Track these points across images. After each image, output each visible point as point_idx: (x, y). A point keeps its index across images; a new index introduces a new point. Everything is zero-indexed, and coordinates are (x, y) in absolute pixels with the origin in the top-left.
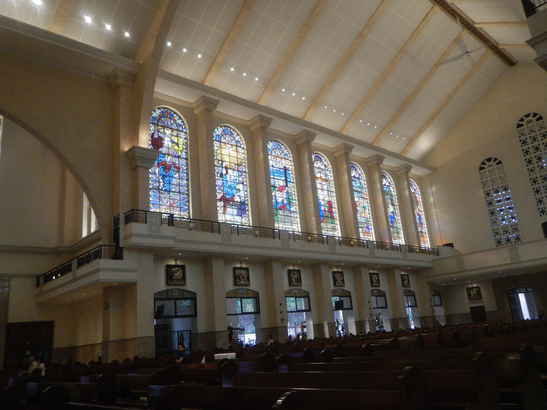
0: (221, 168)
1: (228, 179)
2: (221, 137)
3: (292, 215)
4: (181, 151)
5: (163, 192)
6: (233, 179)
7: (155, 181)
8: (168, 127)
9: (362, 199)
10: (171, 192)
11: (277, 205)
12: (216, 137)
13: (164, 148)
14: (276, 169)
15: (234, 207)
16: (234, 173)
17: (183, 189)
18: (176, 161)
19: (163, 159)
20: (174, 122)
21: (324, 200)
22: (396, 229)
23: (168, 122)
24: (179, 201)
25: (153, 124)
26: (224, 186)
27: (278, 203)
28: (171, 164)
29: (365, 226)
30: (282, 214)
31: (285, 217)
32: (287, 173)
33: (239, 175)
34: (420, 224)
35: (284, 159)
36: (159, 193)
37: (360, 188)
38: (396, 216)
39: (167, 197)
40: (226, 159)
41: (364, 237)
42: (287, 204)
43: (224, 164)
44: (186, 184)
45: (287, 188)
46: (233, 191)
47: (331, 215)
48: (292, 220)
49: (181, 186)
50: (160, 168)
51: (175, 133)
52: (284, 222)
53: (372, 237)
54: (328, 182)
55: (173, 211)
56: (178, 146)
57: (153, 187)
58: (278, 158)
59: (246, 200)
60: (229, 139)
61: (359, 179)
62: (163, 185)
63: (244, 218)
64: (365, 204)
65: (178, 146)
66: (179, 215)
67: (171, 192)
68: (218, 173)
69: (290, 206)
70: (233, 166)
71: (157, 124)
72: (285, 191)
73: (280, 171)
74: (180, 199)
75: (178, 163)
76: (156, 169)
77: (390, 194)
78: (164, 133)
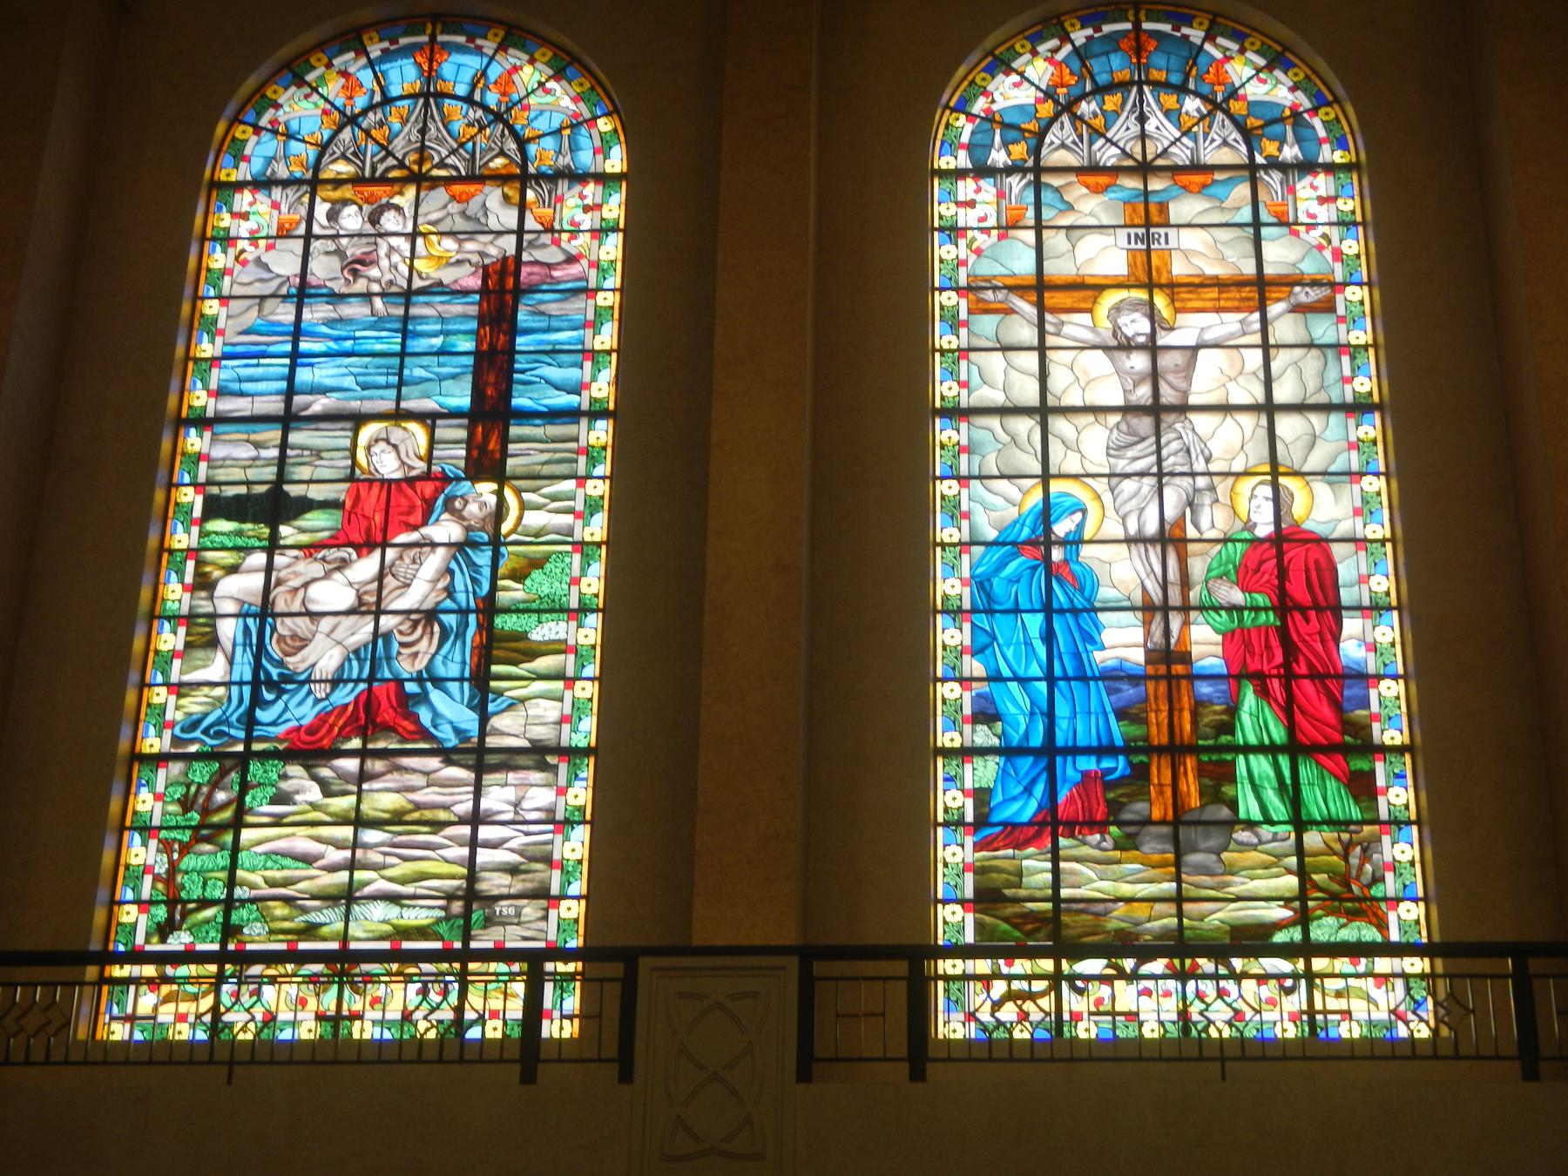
11: (257, 701)
21: (1170, 539)
30: (314, 806)
31: (370, 836)
35: (501, 178)
42: (438, 682)
45: (486, 489)
47: (1288, 711)
48: (483, 856)
72: (445, 530)
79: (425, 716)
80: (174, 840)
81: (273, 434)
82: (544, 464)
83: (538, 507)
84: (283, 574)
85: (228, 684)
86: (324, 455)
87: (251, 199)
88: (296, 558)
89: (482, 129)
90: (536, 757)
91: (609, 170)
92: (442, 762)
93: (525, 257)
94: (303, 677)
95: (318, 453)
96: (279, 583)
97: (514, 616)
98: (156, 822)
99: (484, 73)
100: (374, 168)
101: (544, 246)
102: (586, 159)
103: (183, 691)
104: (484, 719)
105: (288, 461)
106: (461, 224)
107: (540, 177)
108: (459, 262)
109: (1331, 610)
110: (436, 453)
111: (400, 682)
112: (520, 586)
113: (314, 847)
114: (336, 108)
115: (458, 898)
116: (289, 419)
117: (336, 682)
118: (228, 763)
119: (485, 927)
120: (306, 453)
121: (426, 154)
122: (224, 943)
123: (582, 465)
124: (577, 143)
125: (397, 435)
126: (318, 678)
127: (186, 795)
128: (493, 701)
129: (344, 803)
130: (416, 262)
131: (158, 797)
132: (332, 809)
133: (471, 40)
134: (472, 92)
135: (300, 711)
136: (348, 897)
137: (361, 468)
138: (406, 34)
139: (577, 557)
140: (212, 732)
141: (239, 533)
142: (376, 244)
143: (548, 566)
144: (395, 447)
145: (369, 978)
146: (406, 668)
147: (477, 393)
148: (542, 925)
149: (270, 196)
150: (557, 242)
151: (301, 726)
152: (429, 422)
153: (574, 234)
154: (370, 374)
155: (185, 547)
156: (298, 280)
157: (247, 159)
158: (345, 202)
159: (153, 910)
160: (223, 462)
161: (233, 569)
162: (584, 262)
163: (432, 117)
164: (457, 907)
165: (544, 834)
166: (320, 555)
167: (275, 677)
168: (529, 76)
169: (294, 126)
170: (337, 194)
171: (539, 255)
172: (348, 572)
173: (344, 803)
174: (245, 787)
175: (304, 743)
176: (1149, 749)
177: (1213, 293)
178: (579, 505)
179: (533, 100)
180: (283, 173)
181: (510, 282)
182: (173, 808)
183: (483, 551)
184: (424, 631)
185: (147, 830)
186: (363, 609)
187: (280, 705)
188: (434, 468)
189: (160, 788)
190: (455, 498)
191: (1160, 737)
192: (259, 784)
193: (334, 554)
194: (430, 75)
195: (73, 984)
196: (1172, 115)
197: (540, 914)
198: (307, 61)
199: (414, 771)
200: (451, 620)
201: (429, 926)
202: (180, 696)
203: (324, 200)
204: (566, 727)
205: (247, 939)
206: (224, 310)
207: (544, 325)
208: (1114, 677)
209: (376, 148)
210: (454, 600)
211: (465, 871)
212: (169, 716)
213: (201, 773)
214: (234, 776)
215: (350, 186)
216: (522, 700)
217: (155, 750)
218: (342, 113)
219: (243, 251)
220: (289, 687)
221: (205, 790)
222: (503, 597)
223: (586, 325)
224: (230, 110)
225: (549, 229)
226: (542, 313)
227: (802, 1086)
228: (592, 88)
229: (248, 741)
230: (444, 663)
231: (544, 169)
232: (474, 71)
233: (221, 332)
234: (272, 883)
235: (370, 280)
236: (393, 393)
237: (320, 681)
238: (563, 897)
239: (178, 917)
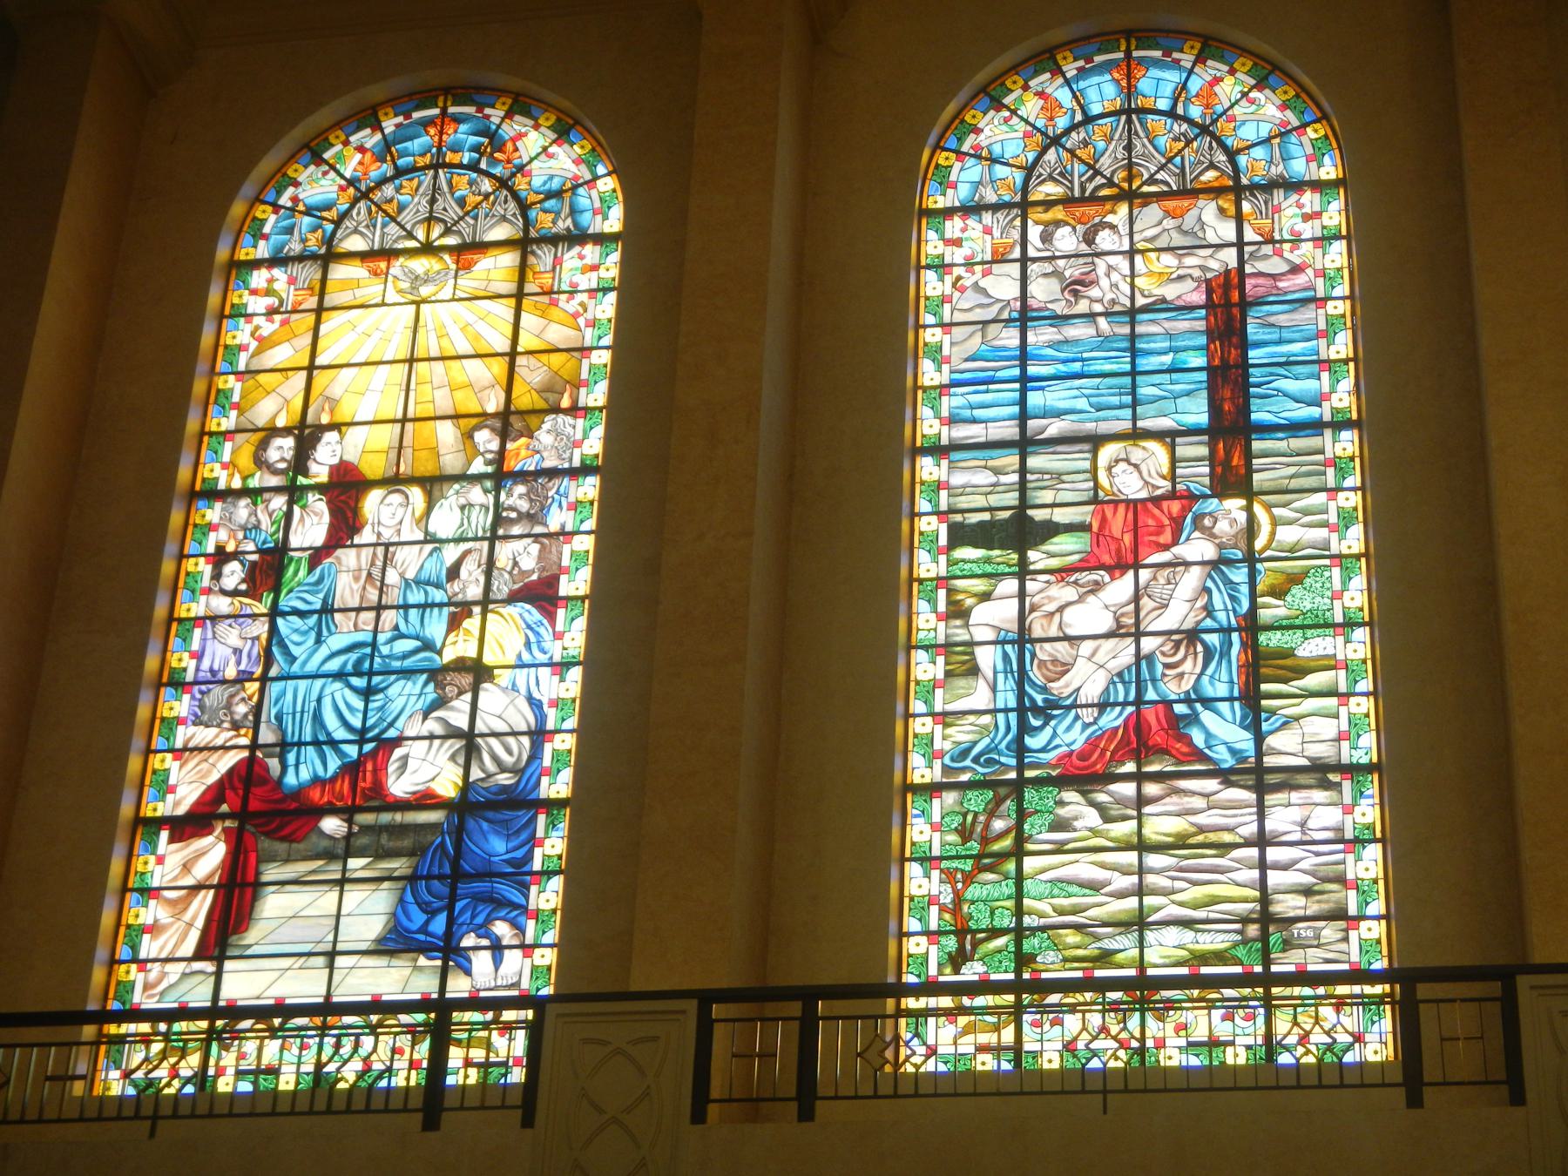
11: (1024, 729)
12: (289, 231)
15: (353, 863)
26: (273, 672)
30: (1095, 832)
31: (1153, 860)
33: (498, 520)
35: (1215, 192)
42: (1208, 702)
45: (1235, 505)
46: (377, 701)
48: (1274, 878)
59: (547, 762)
72: (1197, 548)
79: (1198, 738)
80: (956, 869)
81: (1011, 459)
82: (1292, 477)
83: (1290, 522)
84: (1036, 599)
85: (994, 711)
86: (1064, 478)
87: (962, 225)
88: (1047, 582)
89: (1188, 143)
90: (1318, 776)
91: (1324, 177)
92: (1220, 783)
93: (1248, 269)
94: (1068, 702)
95: (1058, 476)
96: (1033, 609)
97: (1279, 633)
98: (936, 852)
99: (1184, 86)
100: (1083, 189)
101: (1266, 257)
102: (1298, 167)
103: (948, 720)
104: (1259, 739)
105: (1029, 485)
106: (1178, 240)
107: (1253, 187)
108: (1180, 278)
110: (1179, 471)
111: (1168, 704)
112: (1281, 603)
113: (1100, 874)
114: (1039, 130)
115: (1253, 921)
116: (1025, 444)
117: (1103, 706)
118: (1002, 791)
119: (1284, 951)
120: (1046, 477)
121: (1134, 171)
122: (1018, 972)
123: (1331, 477)
124: (1287, 152)
125: (1136, 455)
126: (1084, 702)
127: (963, 824)
128: (1266, 720)
129: (1125, 829)
130: (1138, 281)
131: (935, 827)
132: (1112, 834)
133: (1167, 53)
134: (1175, 106)
135: (1070, 736)
136: (1139, 923)
137: (1103, 489)
138: (1100, 51)
139: (1336, 571)
140: (982, 760)
141: (988, 560)
142: (1093, 263)
143: (1307, 581)
144: (1136, 466)
145: (1170, 1005)
146: (1172, 689)
147: (1214, 408)
148: (1343, 946)
149: (980, 222)
150: (1279, 253)
151: (1072, 751)
152: (1168, 440)
153: (1297, 241)
154: (1103, 395)
155: (934, 575)
156: (1018, 304)
157: (954, 186)
158: (1058, 224)
159: (943, 940)
160: (964, 490)
161: (986, 597)
162: (1310, 272)
163: (1136, 133)
164: (1253, 930)
165: (1334, 855)
166: (1073, 579)
167: (1040, 703)
168: (1229, 89)
169: (997, 149)
170: (1049, 216)
171: (1262, 266)
172: (1101, 594)
173: (1125, 829)
174: (1022, 815)
175: (1078, 768)
178: (1333, 519)
179: (1237, 110)
180: (991, 197)
181: (1235, 296)
182: (953, 838)
183: (1238, 568)
184: (1187, 651)
185: (928, 861)
186: (1122, 631)
187: (1048, 731)
188: (1178, 487)
189: (936, 818)
190: (1203, 515)
192: (1037, 812)
193: (1086, 577)
194: (1130, 91)
195: (876, 1017)
197: (1340, 935)
198: (1003, 84)
199: (1194, 793)
200: (1213, 639)
201: (1226, 950)
202: (946, 725)
203: (1037, 223)
204: (1345, 745)
205: (1042, 967)
206: (947, 338)
207: (1275, 337)
209: (1083, 168)
210: (1214, 619)
211: (1257, 894)
212: (937, 746)
213: (977, 801)
214: (1009, 805)
215: (1060, 207)
216: (1297, 719)
217: (927, 780)
218: (1044, 134)
219: (959, 278)
220: (1055, 712)
221: (982, 818)
222: (1265, 615)
223: (1320, 334)
224: (932, 139)
225: (1270, 240)
226: (1273, 325)
227: (1413, 1111)
228: (1297, 96)
229: (1020, 768)
230: (1212, 684)
231: (1257, 179)
232: (1174, 85)
233: (947, 360)
234: (1061, 912)
235: (1092, 300)
236: (1128, 413)
237: (1087, 706)
238: (1362, 917)
239: (968, 947)
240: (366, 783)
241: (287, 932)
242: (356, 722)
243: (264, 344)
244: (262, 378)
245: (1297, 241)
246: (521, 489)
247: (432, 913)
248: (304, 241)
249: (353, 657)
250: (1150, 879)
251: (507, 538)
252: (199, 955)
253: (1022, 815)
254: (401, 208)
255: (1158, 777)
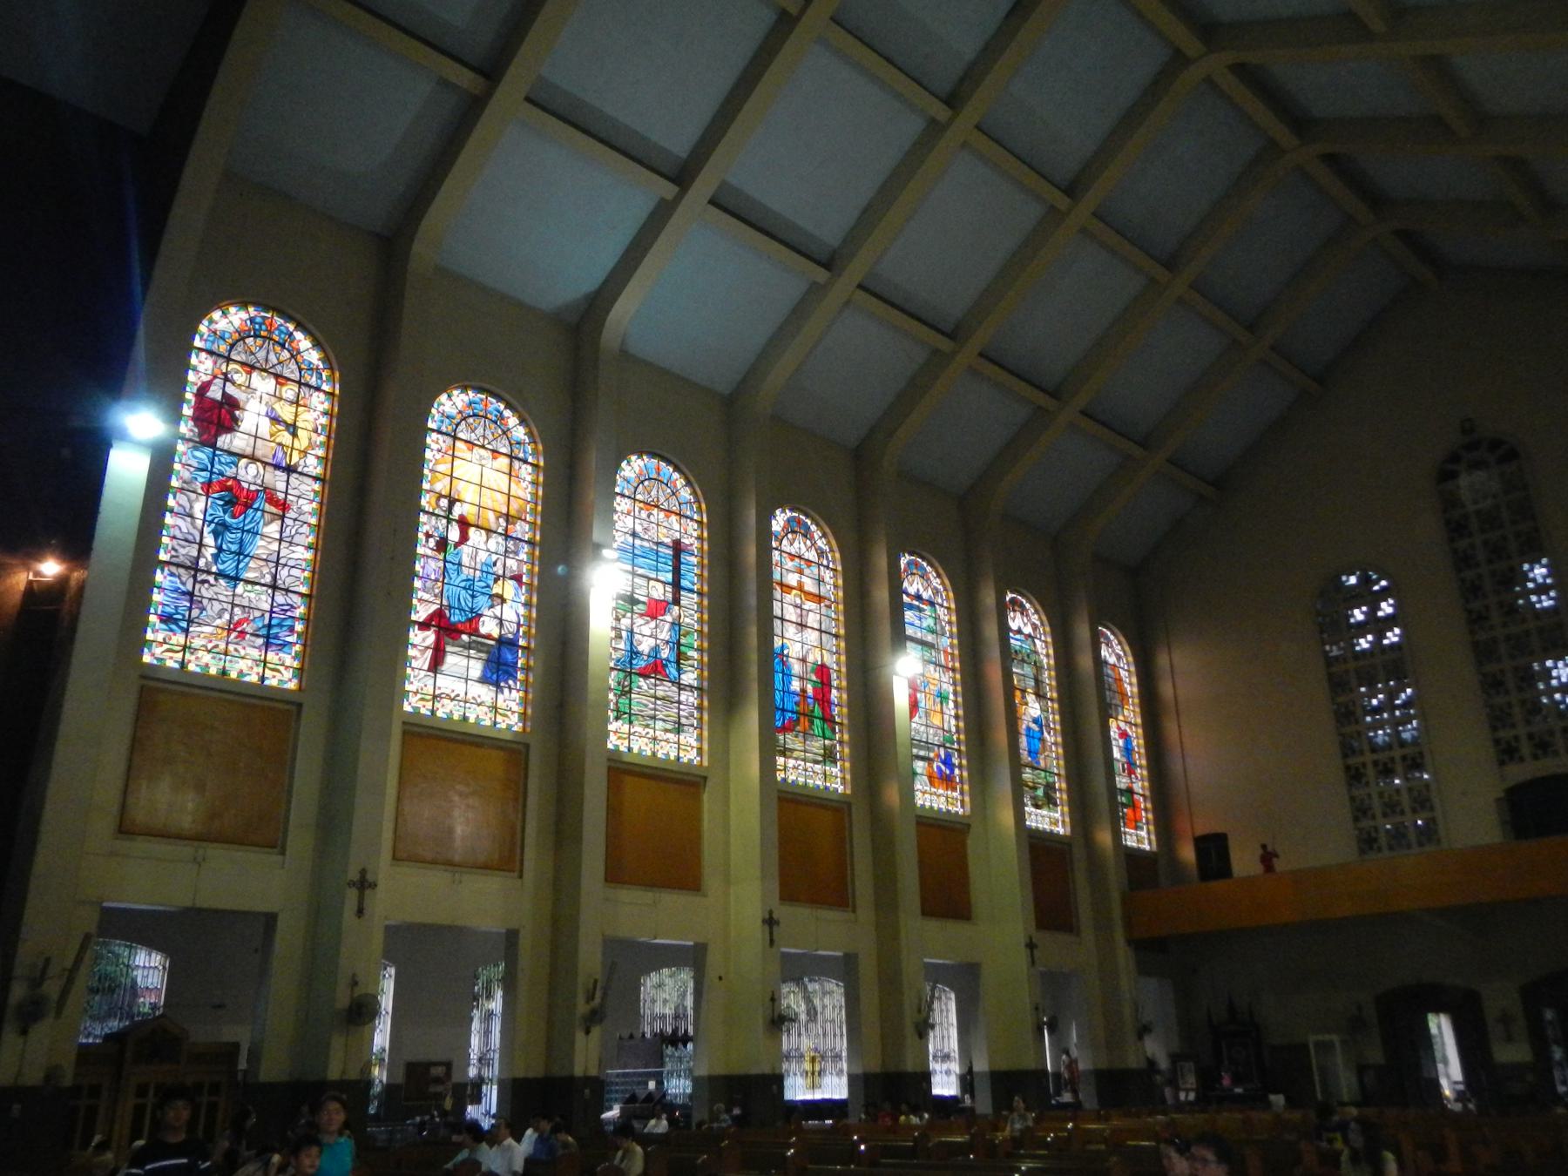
0: (444, 521)
1: (466, 561)
2: (457, 425)
3: (683, 698)
4: (304, 453)
5: (211, 579)
6: (483, 561)
7: (186, 540)
8: (265, 370)
9: (938, 668)
10: (242, 580)
11: (632, 658)
12: (442, 422)
13: (238, 434)
14: (646, 544)
15: (472, 652)
16: (490, 540)
17: (289, 575)
18: (278, 480)
19: (227, 468)
20: (292, 356)
21: (803, 660)
22: (1043, 774)
23: (268, 353)
24: (267, 616)
25: (210, 353)
27: (637, 653)
28: (258, 491)
29: (939, 756)
30: (646, 691)
31: (658, 702)
32: (682, 560)
33: (506, 551)
34: (1126, 766)
35: (676, 514)
36: (195, 581)
37: (933, 632)
38: (1049, 733)
39: (222, 598)
40: (467, 493)
41: (933, 790)
42: (670, 662)
43: (457, 510)
44: (305, 560)
45: (677, 608)
46: (476, 600)
47: (823, 710)
48: (681, 713)
49: (285, 565)
50: (210, 500)
51: (289, 391)
52: (654, 718)
53: (962, 793)
54: (822, 605)
55: (239, 648)
56: (294, 435)
57: (174, 560)
58: (656, 509)
60: (488, 432)
61: (932, 604)
62: (216, 557)
63: (506, 691)
64: (945, 686)
65: (294, 435)
66: (260, 661)
67: (242, 580)
68: (428, 536)
69: (679, 670)
70: (488, 520)
71: (226, 354)
72: (668, 618)
73: (657, 551)
74: (272, 606)
75: (284, 490)
76: (197, 499)
77: (1035, 662)
78: (248, 387)
109: (830, 686)
111: (662, 660)
117: (649, 656)
135: (640, 663)
164: (677, 726)
174: (631, 682)
176: (800, 714)
177: (811, 597)
191: (802, 712)
196: (805, 543)
208: (794, 693)
212: (613, 657)
229: (631, 668)
240: (474, 626)
241: (452, 669)
242: (470, 605)
243: (437, 462)
244: (437, 474)
245: (692, 536)
246: (512, 542)
247: (493, 674)
248: (447, 428)
249: (468, 583)
250: (657, 707)
251: (508, 557)
252: (429, 670)
253: (631, 682)
254: (476, 428)
255: (658, 679)
